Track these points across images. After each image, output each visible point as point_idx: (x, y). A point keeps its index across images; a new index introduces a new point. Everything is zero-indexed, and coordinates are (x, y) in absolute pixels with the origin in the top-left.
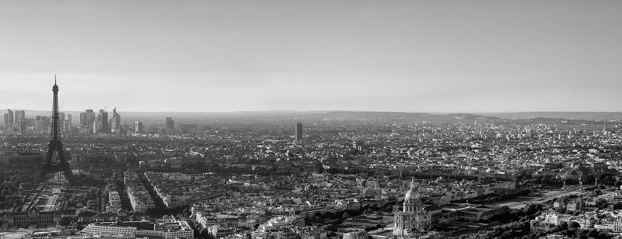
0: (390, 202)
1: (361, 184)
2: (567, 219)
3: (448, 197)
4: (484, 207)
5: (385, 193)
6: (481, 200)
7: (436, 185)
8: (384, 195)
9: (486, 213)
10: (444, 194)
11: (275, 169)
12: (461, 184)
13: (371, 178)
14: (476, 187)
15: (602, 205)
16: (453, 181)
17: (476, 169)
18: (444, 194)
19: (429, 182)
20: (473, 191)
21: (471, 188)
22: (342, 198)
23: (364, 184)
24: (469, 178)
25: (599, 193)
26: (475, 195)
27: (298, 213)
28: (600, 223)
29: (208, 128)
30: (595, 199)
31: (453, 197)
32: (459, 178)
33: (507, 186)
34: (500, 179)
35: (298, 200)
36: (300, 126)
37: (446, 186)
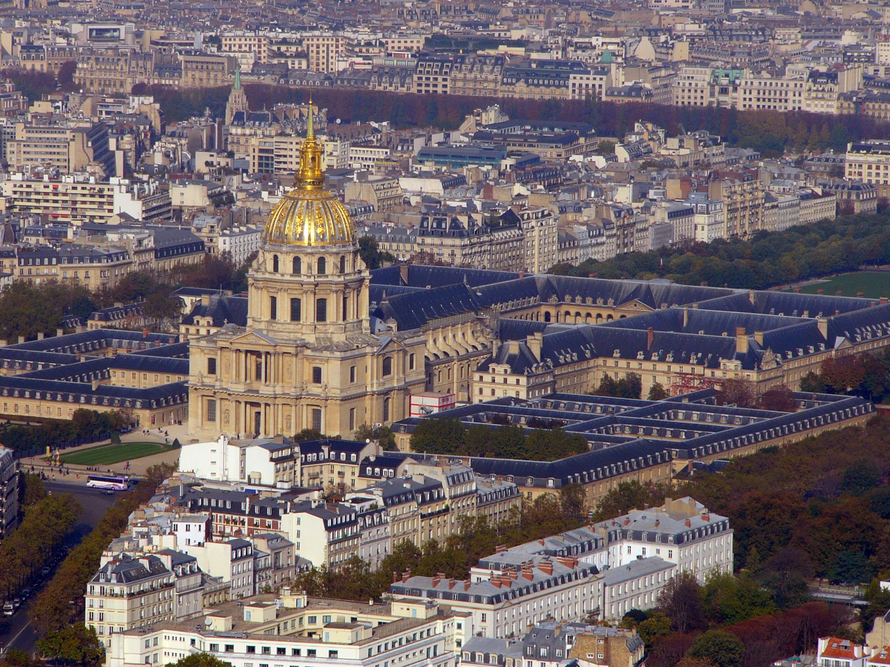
5: (135, 209)
7: (458, 157)
12: (622, 154)
13: (42, 107)
18: (512, 220)
19: (419, 144)
20: (696, 199)
24: (675, 120)
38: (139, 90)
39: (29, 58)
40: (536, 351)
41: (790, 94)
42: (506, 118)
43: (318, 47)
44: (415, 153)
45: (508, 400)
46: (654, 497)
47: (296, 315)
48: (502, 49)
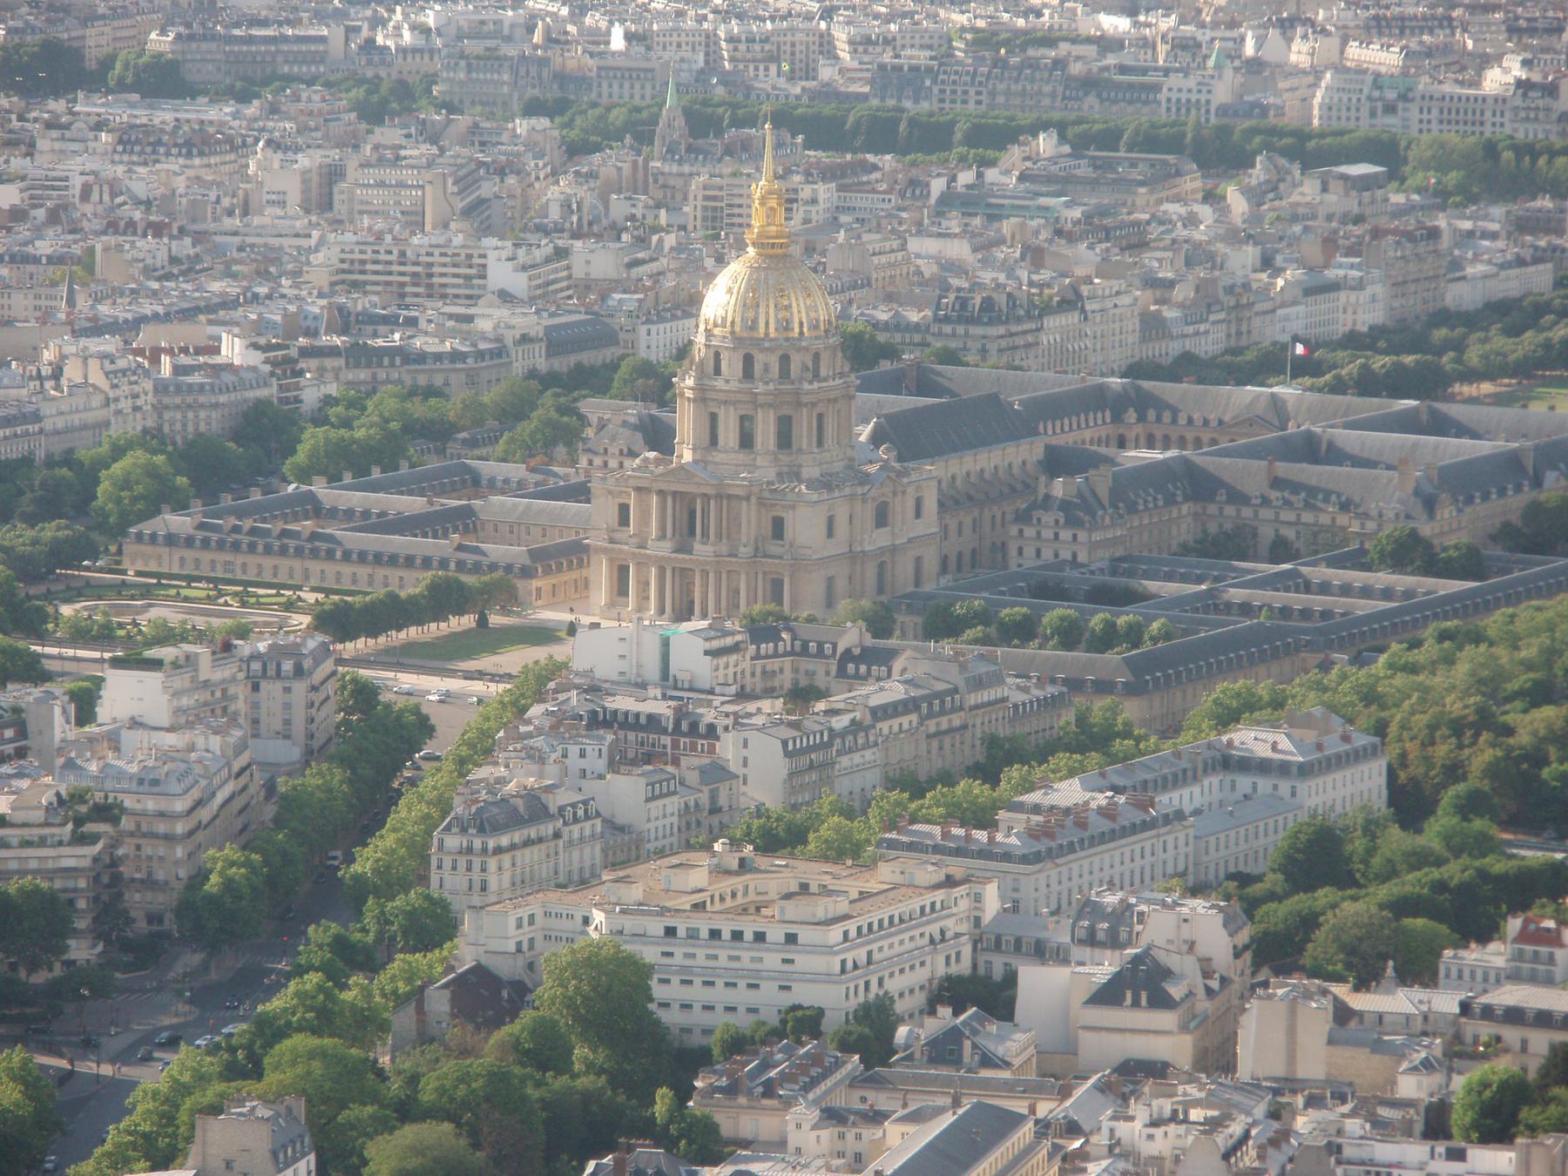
0: (563, 364)
1: (294, 197)
3: (1109, 324)
4: (1441, 426)
5: (518, 283)
8: (504, 305)
9: (1464, 482)
10: (1071, 301)
12: (1237, 203)
13: (388, 134)
14: (1377, 234)
16: (1162, 178)
17: (1383, 57)
18: (1071, 301)
19: (938, 186)
20: (1342, 268)
21: (1330, 244)
22: (113, 327)
26: (1365, 307)
31: (1152, 326)
32: (1221, 152)
37: (1095, 227)
38: (533, 109)
39: (369, 62)
40: (1103, 491)
41: (1488, 114)
42: (1067, 149)
43: (793, 45)
44: (933, 200)
45: (1060, 565)
47: (746, 441)
48: (1064, 48)
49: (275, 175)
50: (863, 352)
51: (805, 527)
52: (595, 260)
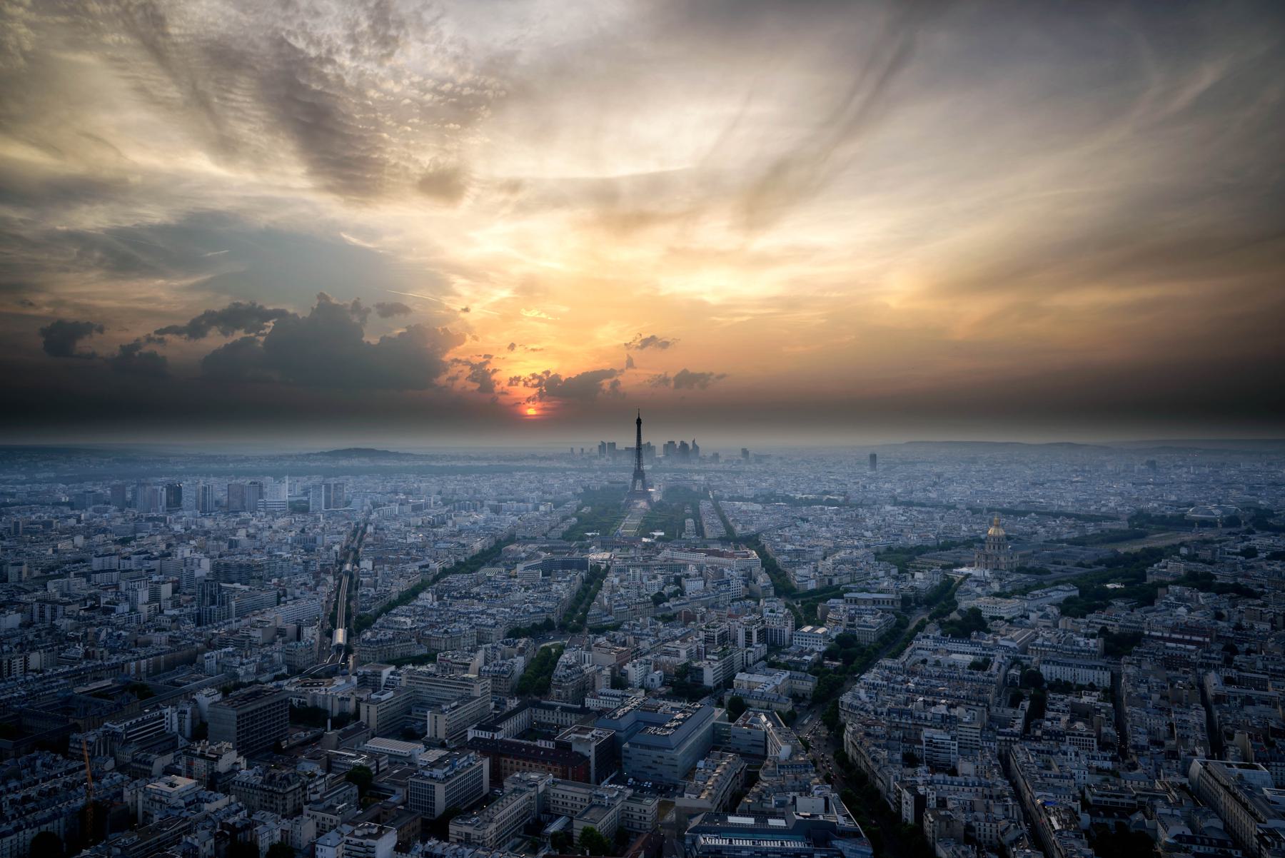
2: (1200, 567)
6: (1080, 542)
11: (847, 500)
15: (1250, 553)
23: (942, 519)
24: (1069, 516)
25: (1244, 539)
26: (1076, 535)
27: (868, 546)
28: (1245, 576)
29: (781, 458)
30: (1239, 546)
32: (1056, 515)
33: (1116, 526)
34: (1107, 518)
35: (868, 534)
36: (873, 457)
46: (1063, 583)
49: (937, 516)
50: (1009, 538)
51: (1002, 559)
52: (975, 527)
